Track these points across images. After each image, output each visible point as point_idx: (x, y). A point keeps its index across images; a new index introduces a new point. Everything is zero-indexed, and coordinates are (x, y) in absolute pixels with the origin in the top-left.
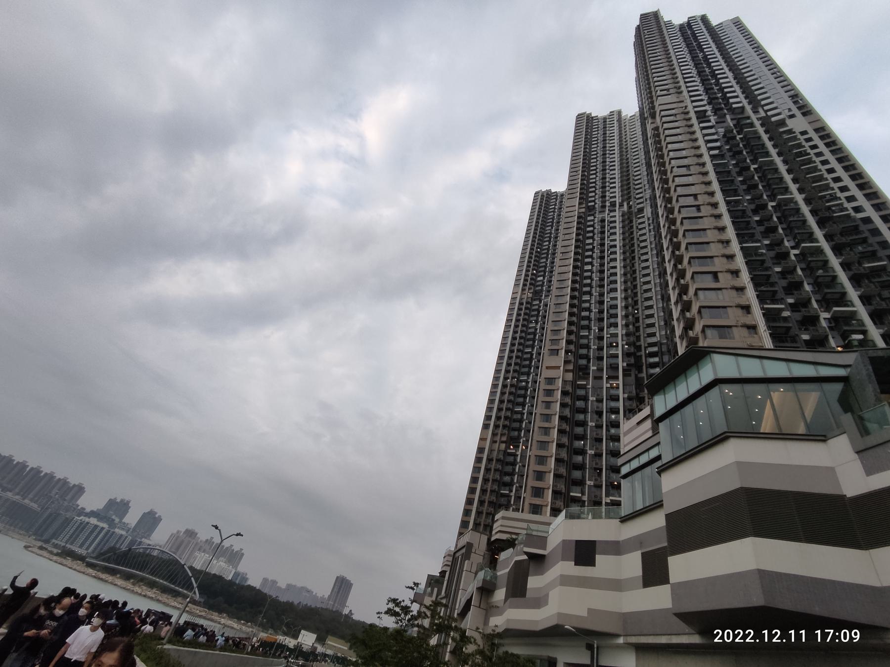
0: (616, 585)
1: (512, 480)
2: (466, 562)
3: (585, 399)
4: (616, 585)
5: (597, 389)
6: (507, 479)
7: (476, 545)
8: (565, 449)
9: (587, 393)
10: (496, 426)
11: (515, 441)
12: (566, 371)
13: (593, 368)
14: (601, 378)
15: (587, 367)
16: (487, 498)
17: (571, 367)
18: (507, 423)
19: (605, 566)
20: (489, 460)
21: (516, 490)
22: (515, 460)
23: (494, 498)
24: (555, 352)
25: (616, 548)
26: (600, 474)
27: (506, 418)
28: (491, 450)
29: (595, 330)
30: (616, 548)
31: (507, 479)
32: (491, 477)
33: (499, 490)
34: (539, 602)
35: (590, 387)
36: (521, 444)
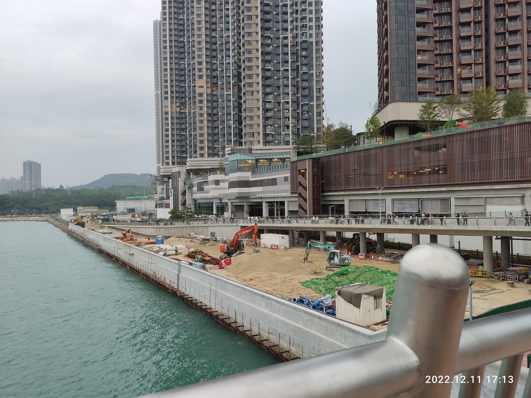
1: (186, 126)
2: (179, 178)
3: (217, 101)
5: (222, 96)
6: (183, 126)
7: (181, 171)
8: (210, 128)
9: (218, 98)
10: (172, 98)
11: (183, 104)
12: (207, 88)
13: (220, 83)
15: (217, 83)
16: (175, 138)
17: (209, 85)
18: (178, 95)
20: (172, 118)
21: (189, 131)
22: (186, 115)
23: (179, 138)
24: (201, 77)
25: (224, 181)
26: (224, 137)
27: (176, 92)
28: (172, 112)
29: (219, 57)
30: (224, 181)
31: (183, 126)
33: (180, 133)
34: (208, 192)
35: (219, 94)
36: (187, 106)
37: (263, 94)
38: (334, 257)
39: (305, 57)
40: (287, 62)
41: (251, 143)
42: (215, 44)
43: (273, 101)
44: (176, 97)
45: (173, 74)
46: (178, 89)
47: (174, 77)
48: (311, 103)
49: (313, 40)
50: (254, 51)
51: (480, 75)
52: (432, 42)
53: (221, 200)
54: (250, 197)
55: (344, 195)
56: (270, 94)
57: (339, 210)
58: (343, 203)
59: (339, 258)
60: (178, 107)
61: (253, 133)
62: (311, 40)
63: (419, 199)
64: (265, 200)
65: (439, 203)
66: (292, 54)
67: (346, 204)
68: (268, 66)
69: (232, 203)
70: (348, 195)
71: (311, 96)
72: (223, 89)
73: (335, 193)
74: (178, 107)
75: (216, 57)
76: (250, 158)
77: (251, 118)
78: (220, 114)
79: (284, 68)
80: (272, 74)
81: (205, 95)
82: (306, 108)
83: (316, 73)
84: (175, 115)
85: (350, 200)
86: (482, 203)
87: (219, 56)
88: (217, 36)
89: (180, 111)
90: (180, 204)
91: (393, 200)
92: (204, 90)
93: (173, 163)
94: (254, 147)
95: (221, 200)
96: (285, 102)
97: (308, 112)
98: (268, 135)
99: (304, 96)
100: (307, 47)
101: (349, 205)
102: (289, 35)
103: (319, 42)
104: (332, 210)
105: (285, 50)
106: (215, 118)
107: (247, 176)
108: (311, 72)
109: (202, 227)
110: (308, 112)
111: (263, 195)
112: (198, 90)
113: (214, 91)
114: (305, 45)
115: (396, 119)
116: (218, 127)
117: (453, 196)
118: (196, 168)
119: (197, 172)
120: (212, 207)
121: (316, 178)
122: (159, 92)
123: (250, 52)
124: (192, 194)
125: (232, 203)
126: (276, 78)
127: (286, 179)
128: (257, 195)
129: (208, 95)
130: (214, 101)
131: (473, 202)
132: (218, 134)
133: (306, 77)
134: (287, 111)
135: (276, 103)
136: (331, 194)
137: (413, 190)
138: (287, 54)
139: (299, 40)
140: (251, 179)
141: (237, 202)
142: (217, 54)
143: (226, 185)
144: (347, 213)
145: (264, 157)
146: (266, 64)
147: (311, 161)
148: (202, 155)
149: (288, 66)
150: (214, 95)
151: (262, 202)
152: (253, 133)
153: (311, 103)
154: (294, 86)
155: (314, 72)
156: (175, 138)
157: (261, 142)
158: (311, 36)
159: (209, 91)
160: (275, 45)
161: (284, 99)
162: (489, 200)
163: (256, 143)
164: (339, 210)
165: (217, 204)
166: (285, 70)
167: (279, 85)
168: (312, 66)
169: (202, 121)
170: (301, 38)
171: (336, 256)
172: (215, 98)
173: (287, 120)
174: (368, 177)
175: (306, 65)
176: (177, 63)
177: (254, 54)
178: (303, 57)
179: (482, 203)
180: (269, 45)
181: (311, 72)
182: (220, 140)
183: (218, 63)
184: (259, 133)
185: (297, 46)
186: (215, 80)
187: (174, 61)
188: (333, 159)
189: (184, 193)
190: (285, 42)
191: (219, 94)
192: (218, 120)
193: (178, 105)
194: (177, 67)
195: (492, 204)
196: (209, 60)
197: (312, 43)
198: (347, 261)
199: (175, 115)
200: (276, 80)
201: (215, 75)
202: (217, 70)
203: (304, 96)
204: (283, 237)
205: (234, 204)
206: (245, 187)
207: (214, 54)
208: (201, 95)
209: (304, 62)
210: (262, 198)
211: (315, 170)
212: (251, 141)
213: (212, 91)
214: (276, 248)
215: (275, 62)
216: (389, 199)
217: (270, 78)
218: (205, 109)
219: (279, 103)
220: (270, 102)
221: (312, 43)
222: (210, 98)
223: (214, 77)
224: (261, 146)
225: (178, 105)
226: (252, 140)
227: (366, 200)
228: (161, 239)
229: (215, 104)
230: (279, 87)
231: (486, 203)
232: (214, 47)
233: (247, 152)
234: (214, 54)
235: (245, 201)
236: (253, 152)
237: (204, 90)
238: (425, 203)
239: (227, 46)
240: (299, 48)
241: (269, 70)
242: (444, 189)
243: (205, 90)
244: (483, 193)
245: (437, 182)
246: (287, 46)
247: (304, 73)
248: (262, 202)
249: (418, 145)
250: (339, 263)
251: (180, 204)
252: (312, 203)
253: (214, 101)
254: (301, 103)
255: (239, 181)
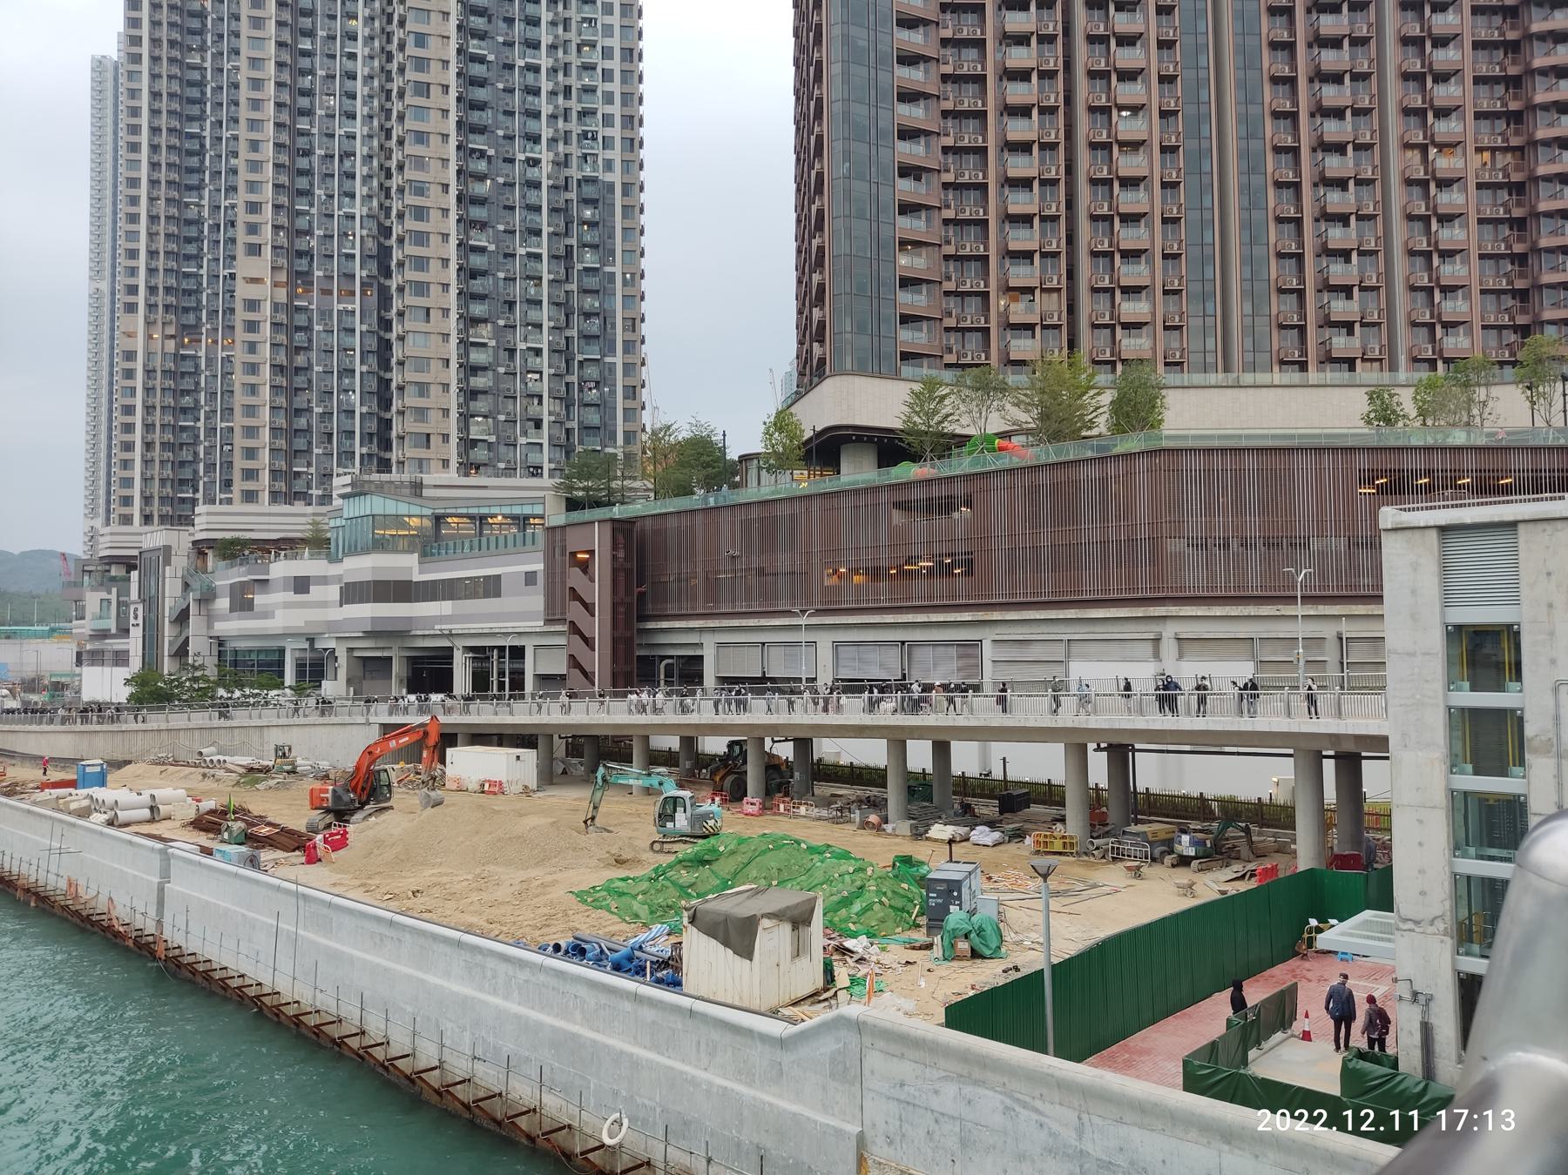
0: (324, 604)
1: (197, 401)
2: (167, 568)
3: (308, 329)
4: (324, 604)
5: (325, 314)
6: (187, 401)
7: (175, 546)
9: (310, 320)
10: (151, 307)
11: (192, 330)
12: (276, 285)
13: (318, 273)
14: (330, 292)
15: (309, 273)
17: (283, 277)
18: (172, 300)
19: (316, 592)
20: (149, 372)
21: (207, 418)
22: (197, 366)
23: (169, 437)
24: (254, 250)
25: (324, 580)
26: (330, 441)
27: (168, 290)
28: (149, 355)
29: (319, 196)
30: (324, 580)
31: (187, 401)
32: (157, 401)
34: (266, 615)
35: (314, 307)
36: (204, 337)
37: (462, 321)
38: (675, 811)
39: (593, 224)
40: (538, 233)
41: (420, 467)
42: (307, 153)
43: (493, 343)
44: (167, 307)
45: (157, 234)
46: (172, 282)
47: (161, 243)
48: (608, 360)
49: (615, 177)
50: (435, 191)
51: (1055, 321)
52: (937, 219)
53: (311, 640)
54: (413, 633)
55: (701, 630)
56: (485, 321)
57: (688, 673)
58: (698, 653)
59: (689, 815)
60: (172, 337)
61: (428, 435)
62: (608, 177)
63: (903, 643)
64: (460, 643)
65: (953, 651)
66: (553, 210)
67: (709, 654)
68: (479, 240)
69: (350, 650)
70: (713, 630)
71: (608, 337)
72: (330, 292)
73: (677, 624)
74: (172, 337)
75: (307, 193)
76: (415, 510)
77: (423, 389)
78: (316, 369)
79: (529, 250)
80: (489, 263)
81: (267, 308)
82: (592, 372)
83: (624, 274)
84: (157, 363)
85: (720, 645)
86: (1058, 652)
87: (317, 192)
88: (315, 131)
89: (177, 350)
90: (166, 653)
91: (837, 645)
92: (263, 292)
93: (147, 519)
94: (427, 479)
95: (311, 640)
96: (529, 349)
97: (597, 383)
98: (474, 443)
99: (587, 338)
100: (596, 195)
101: (717, 657)
102: (544, 154)
103: (632, 188)
104: (669, 674)
105: (532, 196)
106: (300, 381)
107: (407, 566)
108: (608, 269)
109: (244, 731)
110: (597, 383)
111: (457, 628)
112: (243, 291)
113: (298, 297)
114: (589, 191)
115: (845, 422)
116: (310, 410)
117: (988, 636)
118: (228, 535)
119: (231, 550)
120: (281, 663)
121: (622, 578)
122: (105, 286)
123: (420, 191)
124: (210, 619)
125: (350, 650)
126: (501, 275)
127: (530, 578)
128: (437, 627)
129: (276, 307)
130: (299, 329)
131: (1035, 652)
132: (308, 430)
133: (592, 282)
134: (537, 376)
135: (501, 352)
136: (665, 625)
137: (889, 618)
138: (538, 209)
139: (574, 173)
140: (417, 577)
141: (368, 648)
142: (312, 185)
143: (333, 592)
144: (709, 680)
145: (460, 511)
146: (473, 233)
147: (608, 527)
148: (250, 496)
149: (539, 245)
150: (299, 309)
151: (451, 649)
152: (428, 435)
153: (608, 360)
154: (558, 304)
155: (617, 269)
156: (157, 436)
157: (454, 464)
158: (609, 165)
159: (282, 295)
160: (501, 180)
161: (525, 340)
162: (1075, 648)
163: (437, 465)
164: (688, 673)
165: (298, 654)
166: (529, 255)
167: (511, 298)
168: (612, 253)
169: (253, 389)
170: (580, 168)
171: (680, 809)
172: (301, 320)
173: (536, 401)
174: (769, 579)
175: (595, 247)
176: (174, 200)
177: (433, 198)
178: (584, 223)
179: (1058, 652)
180: (481, 178)
181: (608, 269)
182: (316, 451)
183: (314, 211)
184: (446, 438)
185: (566, 188)
186: (302, 264)
187: (163, 191)
188: (672, 523)
189: (182, 618)
190: (532, 173)
191: (314, 307)
192: (310, 388)
193: (171, 330)
194: (174, 211)
195: (1085, 657)
196: (284, 200)
197: (610, 187)
198: (711, 823)
199: (157, 363)
200: (501, 283)
201: (304, 247)
202: (309, 232)
203: (587, 338)
204: (518, 757)
205: (357, 654)
206: (395, 601)
207: (302, 183)
208: (252, 305)
209: (588, 238)
210: (451, 635)
211: (621, 554)
212: (420, 461)
213: (292, 296)
214: (496, 789)
215: (501, 227)
216: (825, 641)
217: (484, 273)
218: (265, 351)
219: (512, 352)
220: (484, 345)
221: (610, 187)
222: (282, 317)
223: (300, 254)
224: (452, 476)
225: (171, 330)
226: (423, 456)
227: (763, 644)
228: (98, 769)
229: (300, 337)
230: (511, 305)
231: (1068, 655)
232: (303, 163)
233: (407, 491)
234: (302, 183)
235: (396, 644)
236: (426, 492)
237: (263, 292)
238: (919, 654)
239: (347, 164)
240: (573, 195)
241: (482, 250)
242: (966, 616)
243: (267, 294)
244: (1061, 628)
245: (948, 598)
246: (537, 185)
247: (586, 270)
248: (451, 649)
249: (901, 496)
250: (688, 830)
251: (166, 653)
252: (608, 651)
253: (299, 329)
254: (579, 357)
255: (375, 582)
